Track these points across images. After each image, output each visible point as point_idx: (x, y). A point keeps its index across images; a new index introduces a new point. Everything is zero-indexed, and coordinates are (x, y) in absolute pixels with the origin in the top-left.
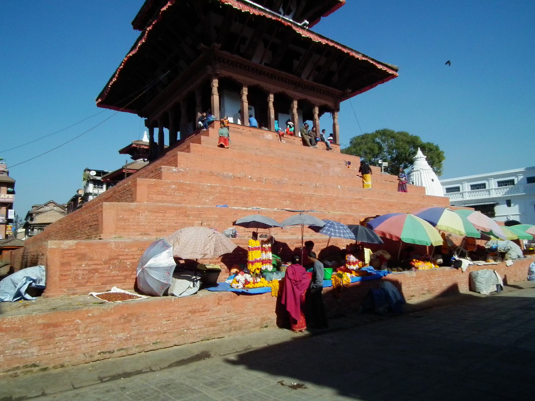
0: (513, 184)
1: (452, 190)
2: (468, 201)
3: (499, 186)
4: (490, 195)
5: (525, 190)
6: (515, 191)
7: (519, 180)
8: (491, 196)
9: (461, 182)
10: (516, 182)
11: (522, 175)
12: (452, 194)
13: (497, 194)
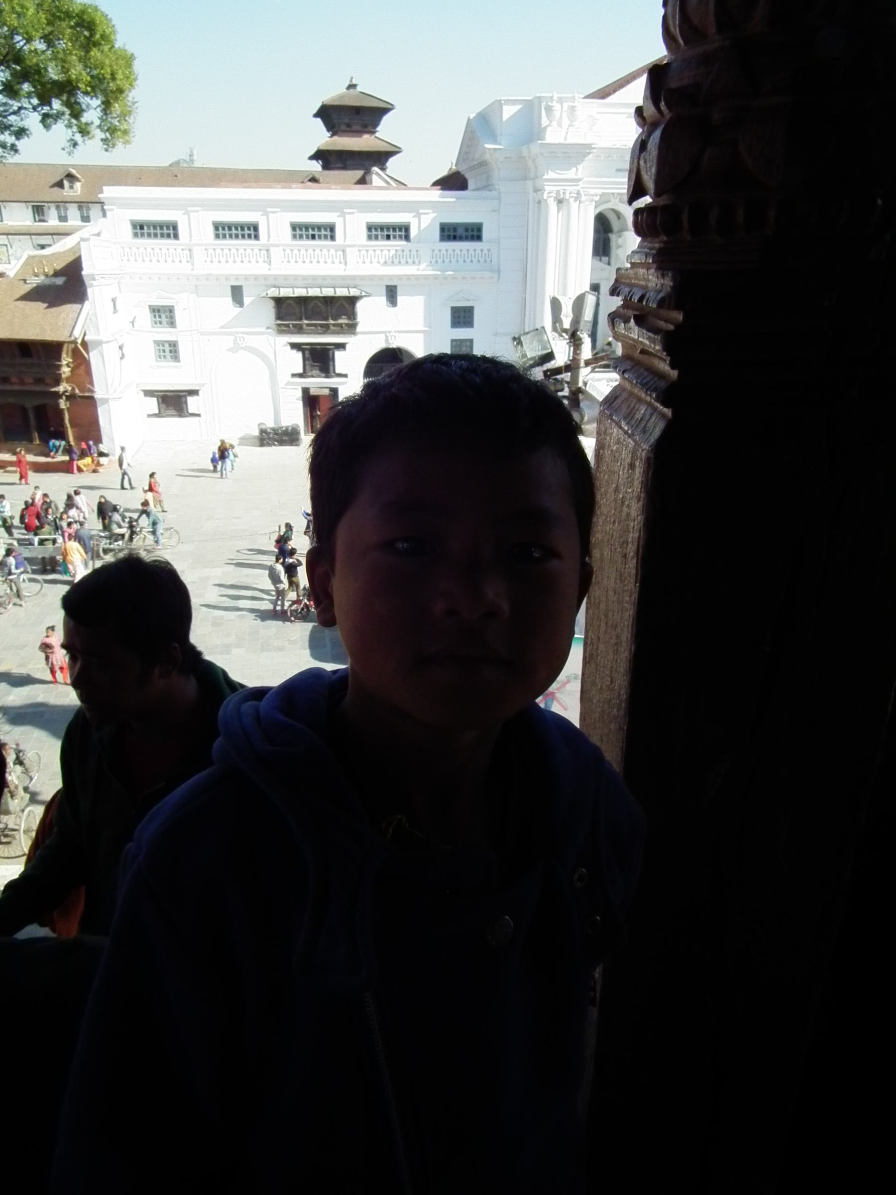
0: (407, 238)
1: (234, 231)
2: (286, 277)
3: (370, 237)
4: (270, 263)
5: (433, 261)
6: (410, 261)
7: (422, 229)
8: (347, 273)
9: (263, 206)
10: (413, 233)
11: (434, 212)
12: (324, 246)
13: (364, 262)
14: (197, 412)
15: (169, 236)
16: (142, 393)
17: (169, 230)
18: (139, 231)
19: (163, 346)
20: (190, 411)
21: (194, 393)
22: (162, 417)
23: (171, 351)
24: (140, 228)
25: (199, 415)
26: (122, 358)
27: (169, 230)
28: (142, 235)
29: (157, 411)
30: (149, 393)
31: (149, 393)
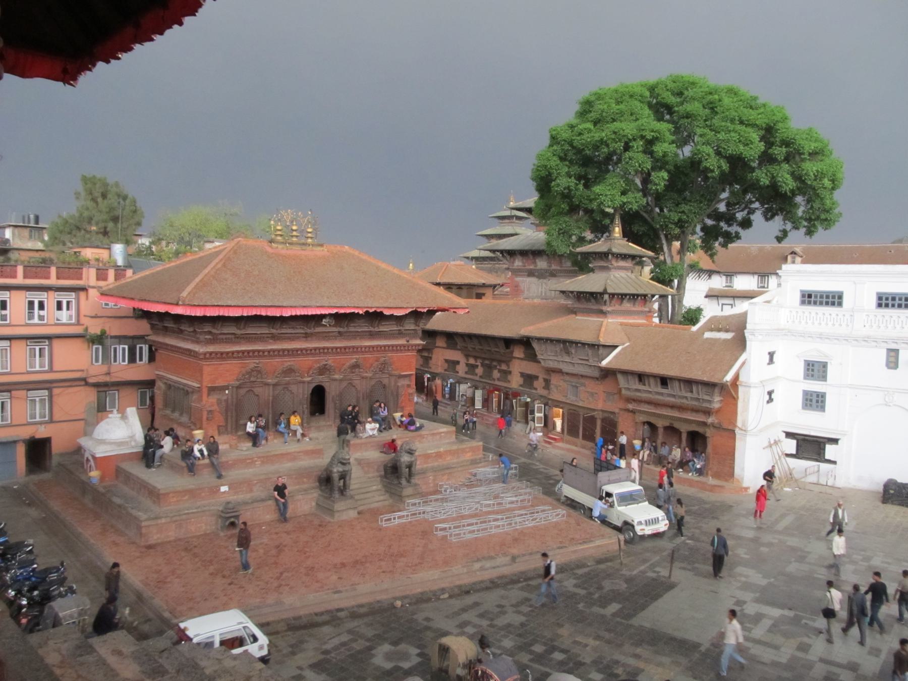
14: (832, 459)
15: (833, 304)
16: (784, 434)
17: (834, 299)
18: (806, 299)
19: (811, 395)
20: (827, 457)
21: (835, 441)
22: (799, 458)
23: (817, 402)
24: (808, 298)
25: (834, 463)
26: (768, 402)
27: (834, 299)
28: (809, 303)
29: (794, 452)
30: (789, 435)
31: (789, 435)
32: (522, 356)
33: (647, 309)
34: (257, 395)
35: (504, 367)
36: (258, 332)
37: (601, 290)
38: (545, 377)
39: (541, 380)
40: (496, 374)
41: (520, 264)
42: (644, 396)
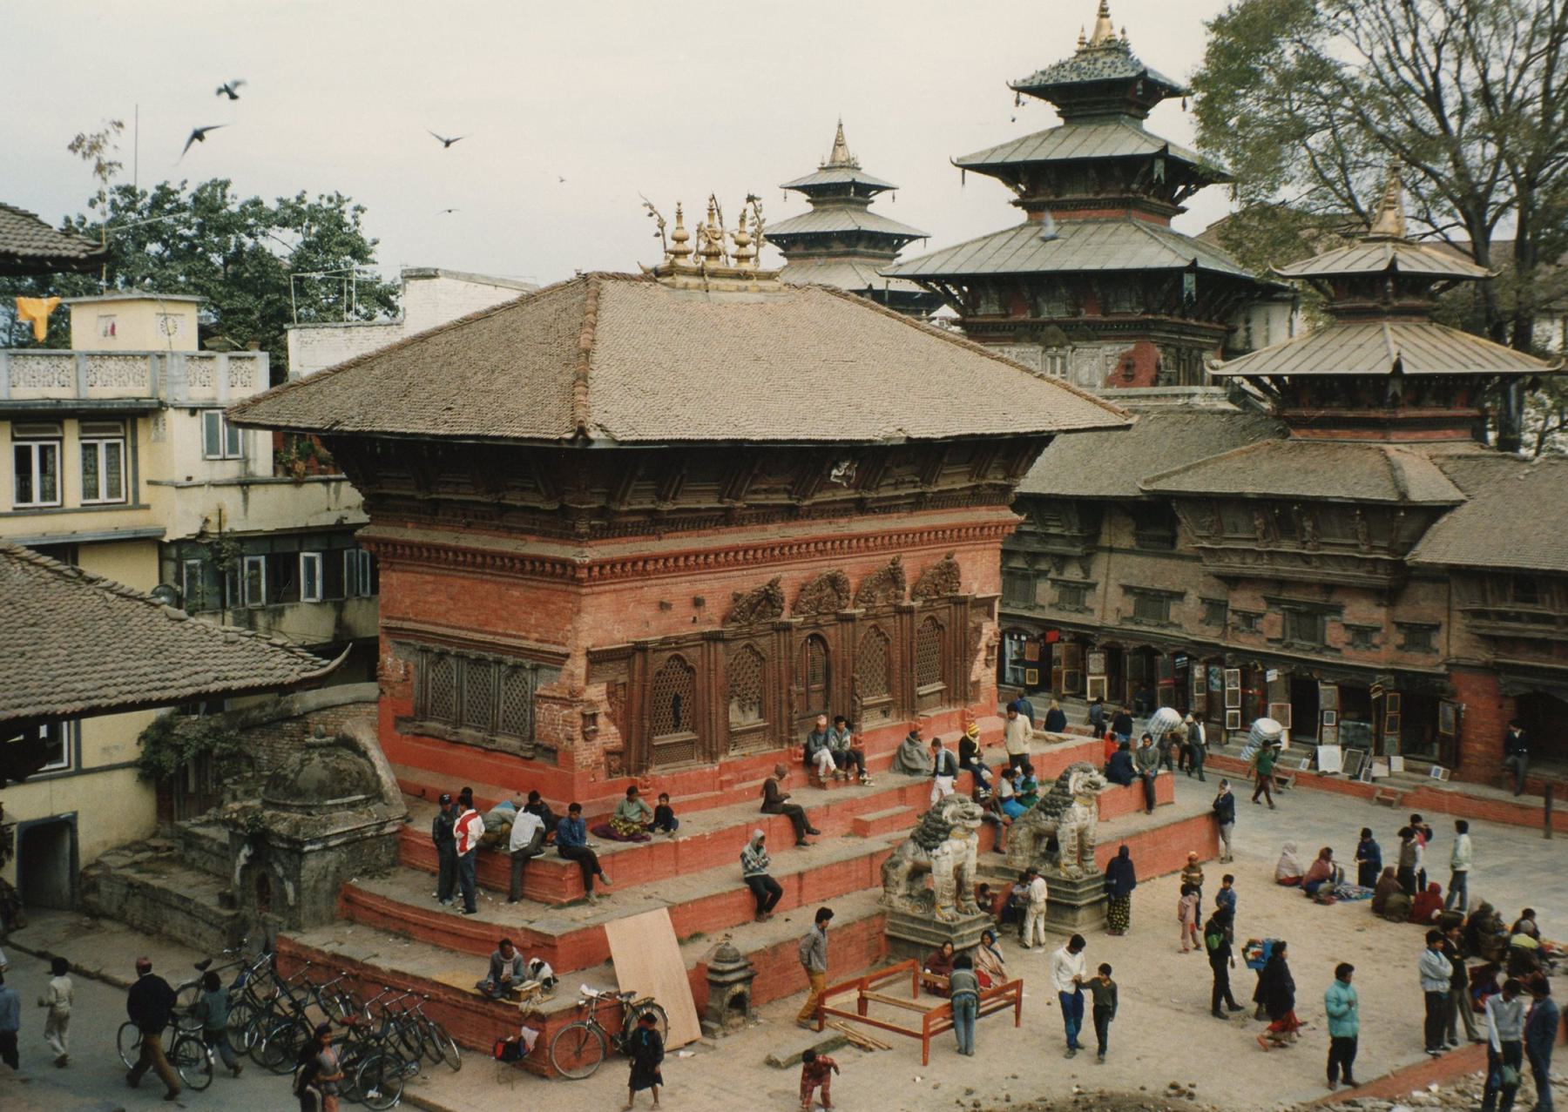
32: (1127, 541)
33: (1474, 412)
34: (690, 670)
35: (1073, 573)
36: (703, 506)
37: (1385, 368)
38: (1215, 594)
39: (1192, 598)
40: (1045, 591)
41: (995, 309)
42: (1535, 631)
